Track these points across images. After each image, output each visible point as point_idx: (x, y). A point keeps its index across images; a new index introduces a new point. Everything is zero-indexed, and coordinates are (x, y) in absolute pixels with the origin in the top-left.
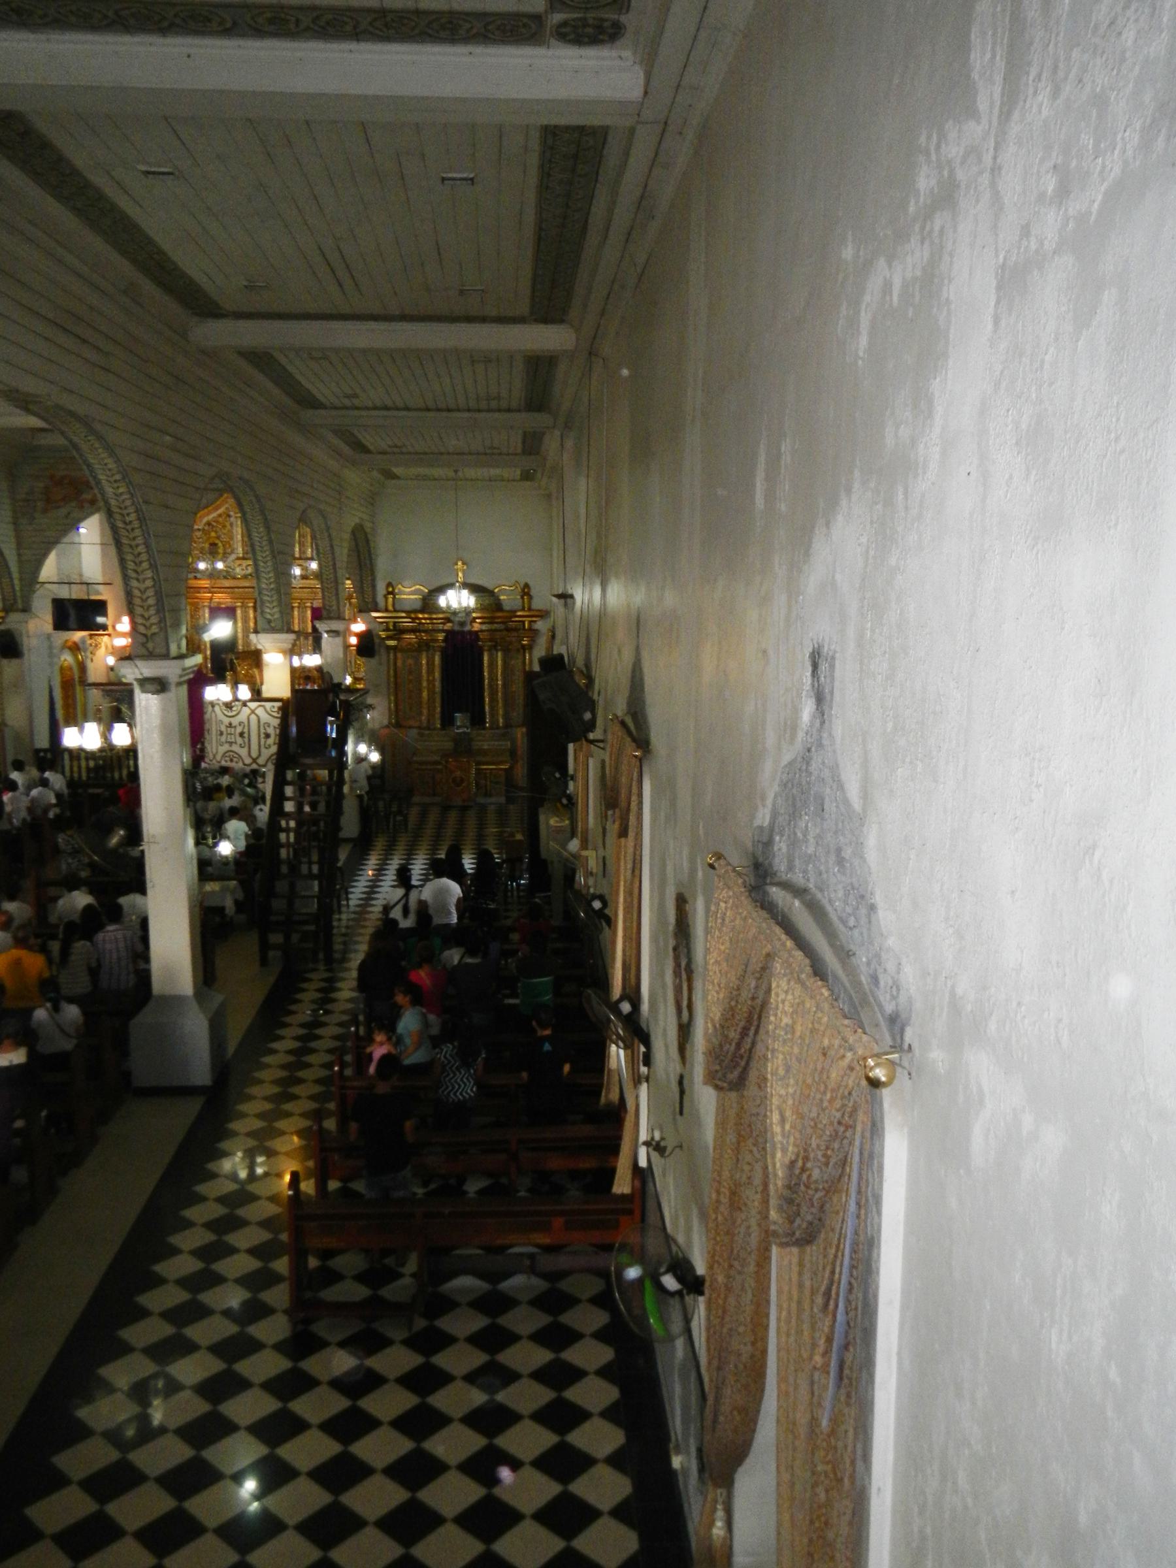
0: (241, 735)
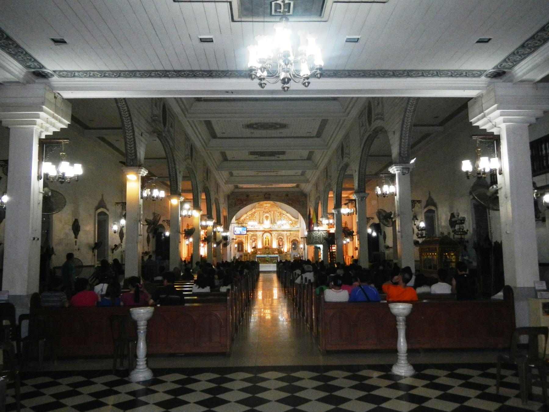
0: (319, 238)
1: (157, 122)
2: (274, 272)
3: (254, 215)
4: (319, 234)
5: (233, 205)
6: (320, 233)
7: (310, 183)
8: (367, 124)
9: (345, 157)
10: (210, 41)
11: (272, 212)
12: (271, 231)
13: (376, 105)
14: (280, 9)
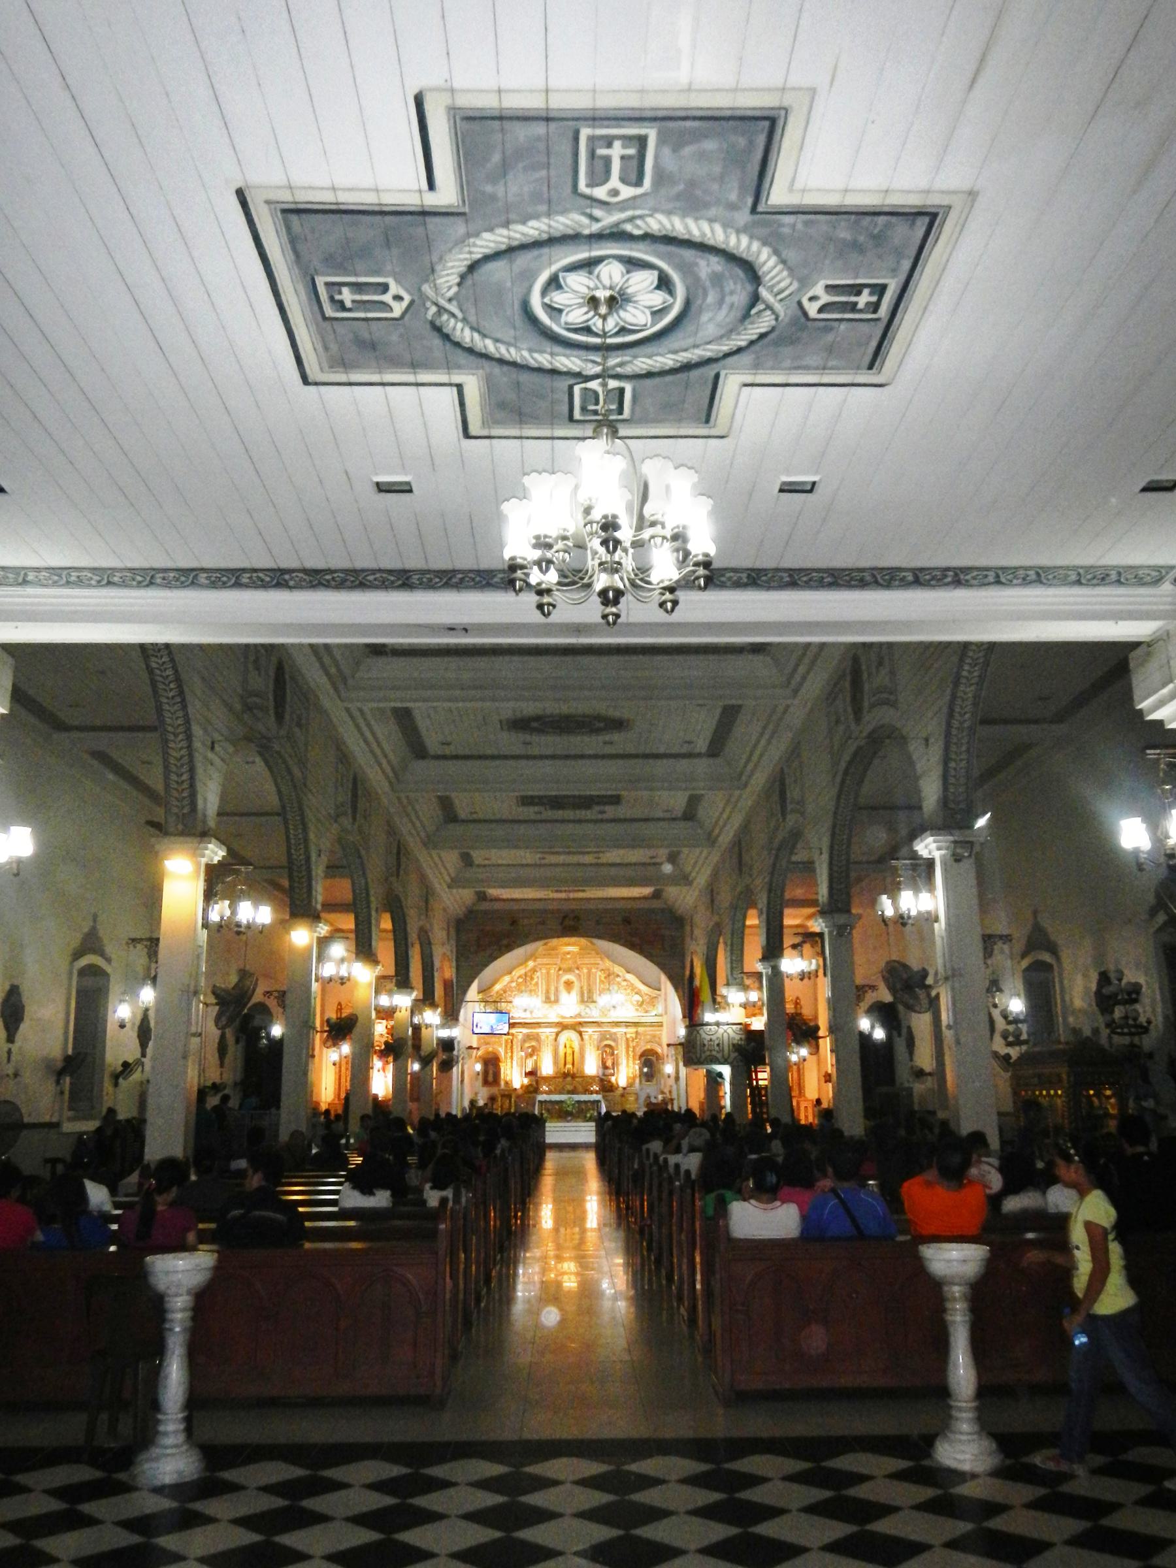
1: (255, 711)
2: (585, 1146)
3: (532, 979)
4: (719, 1034)
6: (721, 1031)
10: (405, 489)
11: (585, 971)
12: (580, 1023)
14: (597, 403)
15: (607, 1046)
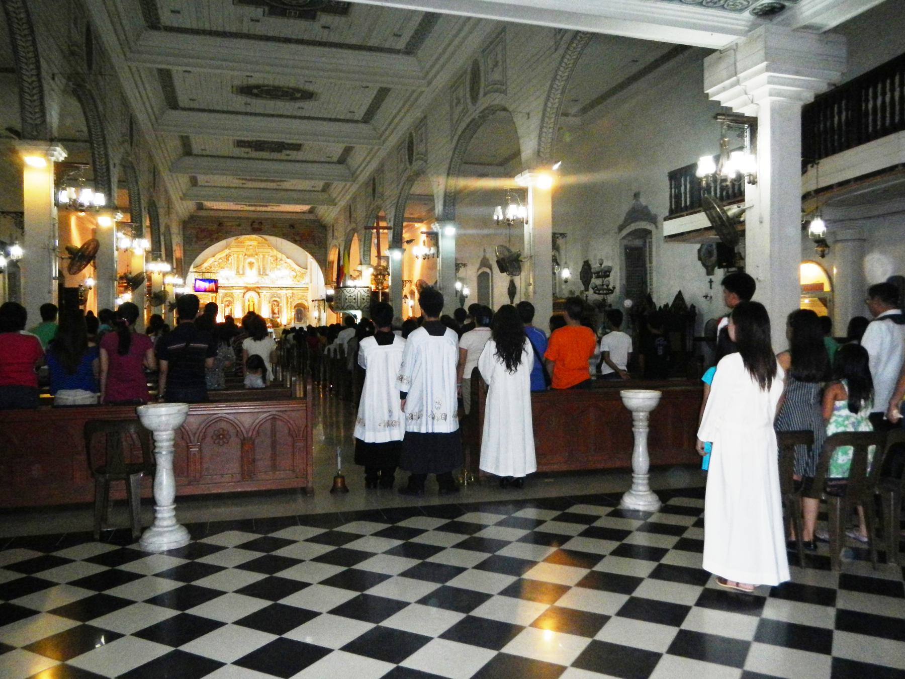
4: (355, 293)
5: (194, 239)
7: (335, 205)
8: (469, 101)
9: (416, 160)
11: (261, 256)
12: (258, 287)
13: (491, 66)
15: (274, 301)
